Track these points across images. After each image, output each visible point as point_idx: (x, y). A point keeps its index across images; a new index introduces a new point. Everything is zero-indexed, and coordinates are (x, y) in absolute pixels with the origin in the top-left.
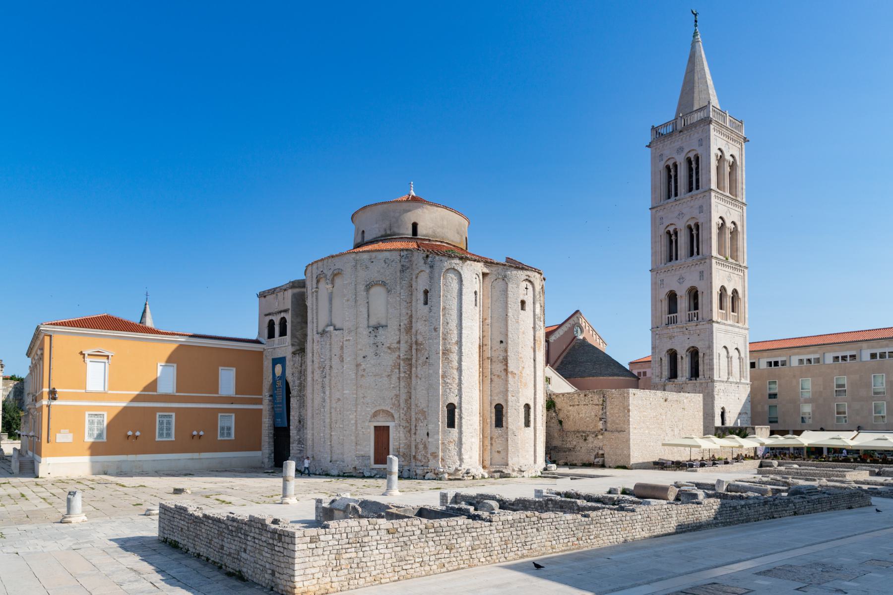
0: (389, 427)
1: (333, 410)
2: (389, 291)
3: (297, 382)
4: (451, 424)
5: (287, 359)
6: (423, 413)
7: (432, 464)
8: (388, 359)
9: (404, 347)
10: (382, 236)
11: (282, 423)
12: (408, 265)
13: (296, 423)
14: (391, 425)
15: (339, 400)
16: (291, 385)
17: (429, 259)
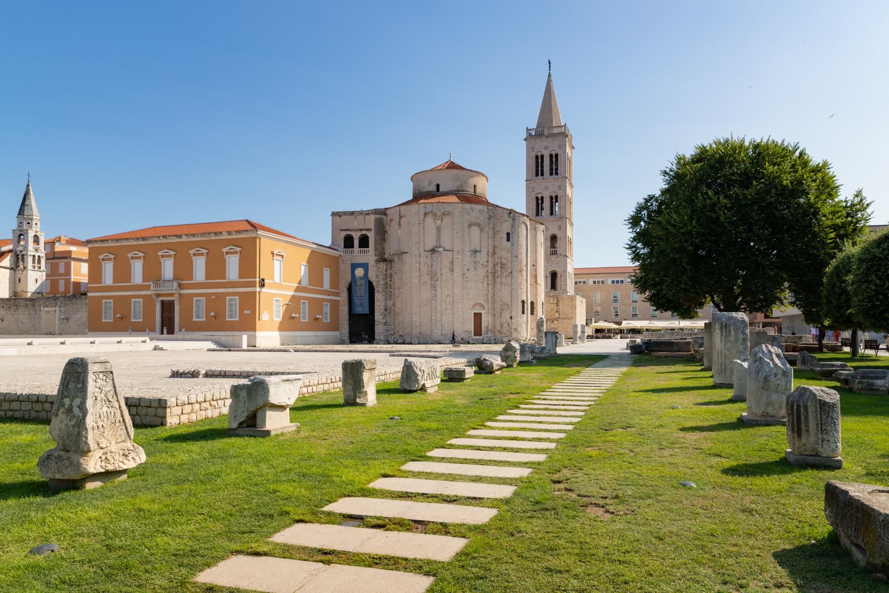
0: (481, 314)
1: (443, 303)
2: (481, 230)
3: (382, 282)
4: (523, 313)
5: (369, 265)
6: (507, 305)
7: (514, 335)
8: (482, 272)
9: (490, 265)
10: (456, 191)
11: (362, 308)
12: (492, 215)
13: (382, 311)
14: (483, 312)
15: (449, 295)
16: (374, 284)
17: (512, 215)
